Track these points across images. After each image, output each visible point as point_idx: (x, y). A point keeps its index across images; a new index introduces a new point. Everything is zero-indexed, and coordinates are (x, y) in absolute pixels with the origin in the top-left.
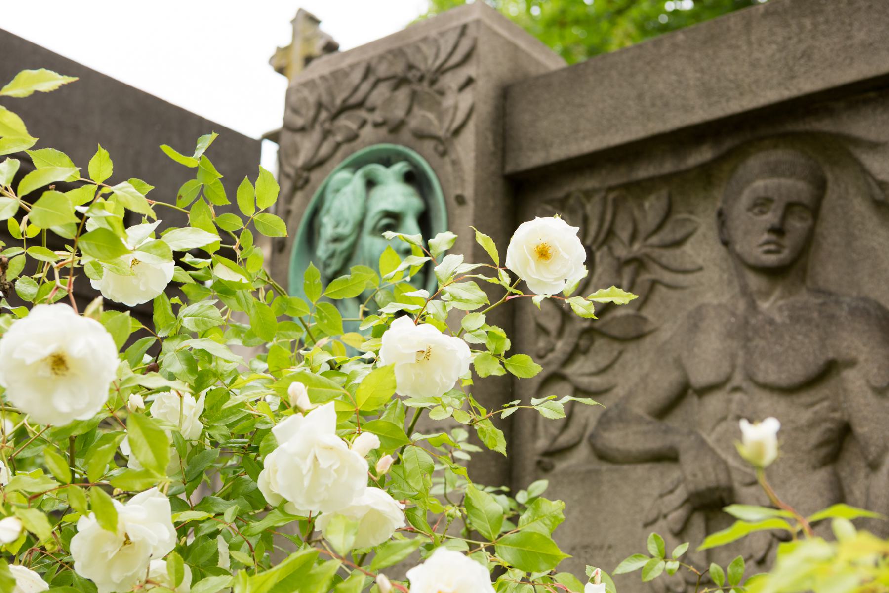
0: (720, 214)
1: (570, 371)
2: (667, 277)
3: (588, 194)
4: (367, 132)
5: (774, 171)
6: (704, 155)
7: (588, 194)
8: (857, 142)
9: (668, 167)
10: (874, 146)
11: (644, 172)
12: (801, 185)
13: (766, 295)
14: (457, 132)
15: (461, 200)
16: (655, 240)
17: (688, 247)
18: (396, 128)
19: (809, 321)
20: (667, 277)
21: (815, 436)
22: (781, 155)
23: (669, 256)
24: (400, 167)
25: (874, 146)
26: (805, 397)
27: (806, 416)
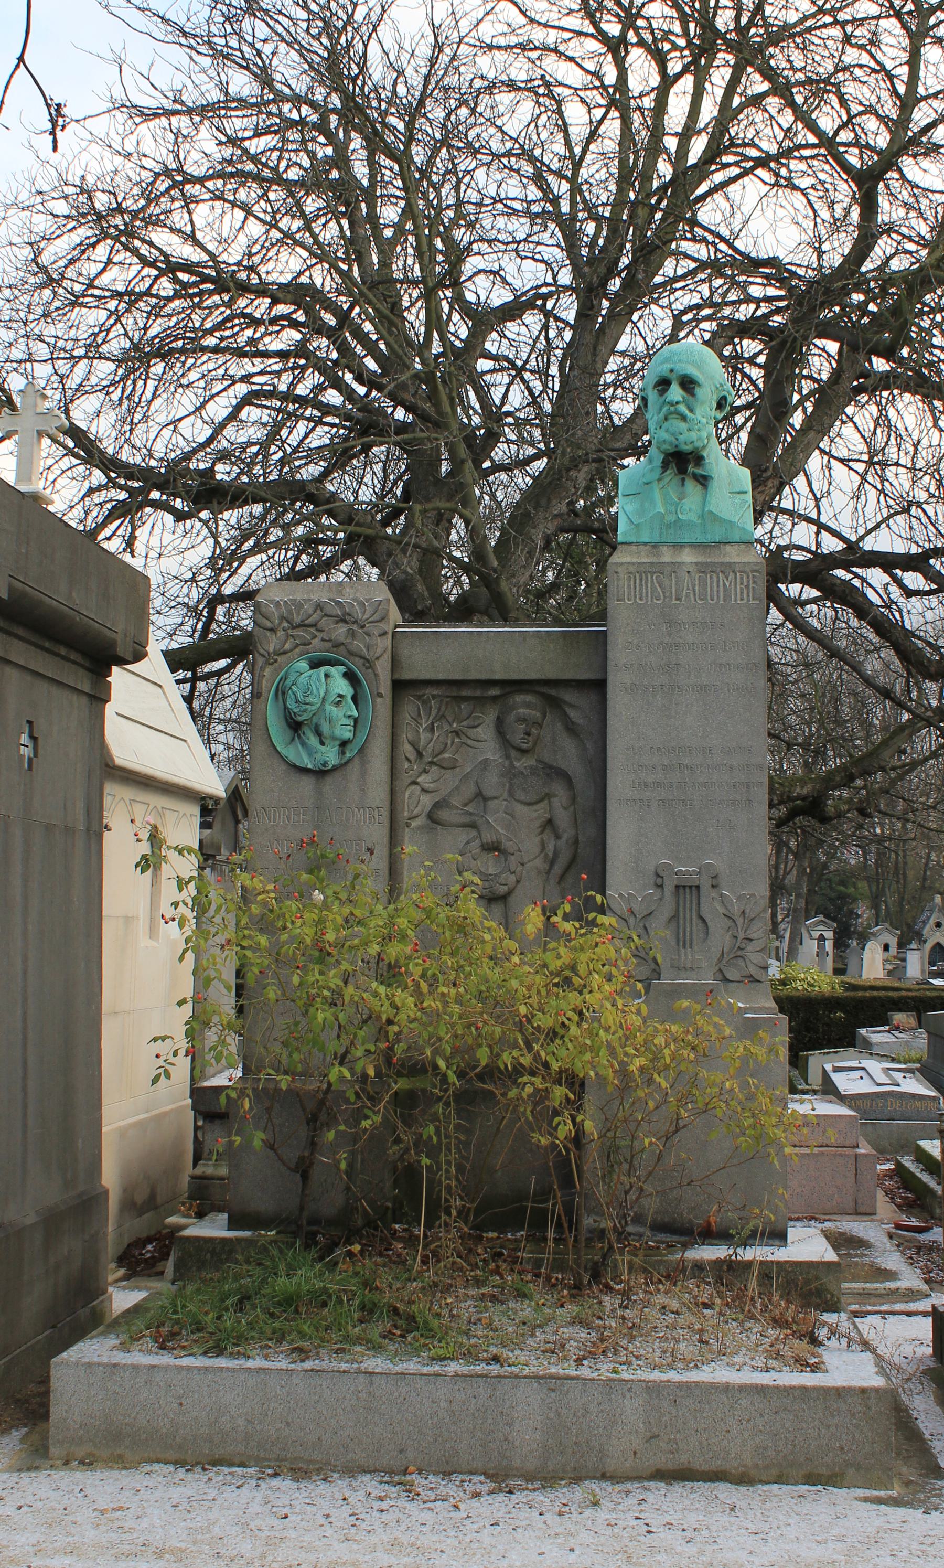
0: (498, 718)
1: (419, 780)
2: (469, 742)
3: (434, 697)
4: (316, 642)
5: (528, 705)
6: (494, 692)
7: (434, 697)
8: (565, 702)
9: (478, 693)
10: (572, 706)
11: (466, 692)
12: (538, 714)
13: (519, 760)
14: (377, 658)
15: (380, 695)
16: (465, 723)
17: (479, 729)
18: (337, 645)
19: (538, 775)
20: (469, 742)
21: (538, 823)
22: (529, 698)
23: (470, 732)
24: (342, 669)
25: (572, 706)
26: (535, 807)
27: (535, 815)
